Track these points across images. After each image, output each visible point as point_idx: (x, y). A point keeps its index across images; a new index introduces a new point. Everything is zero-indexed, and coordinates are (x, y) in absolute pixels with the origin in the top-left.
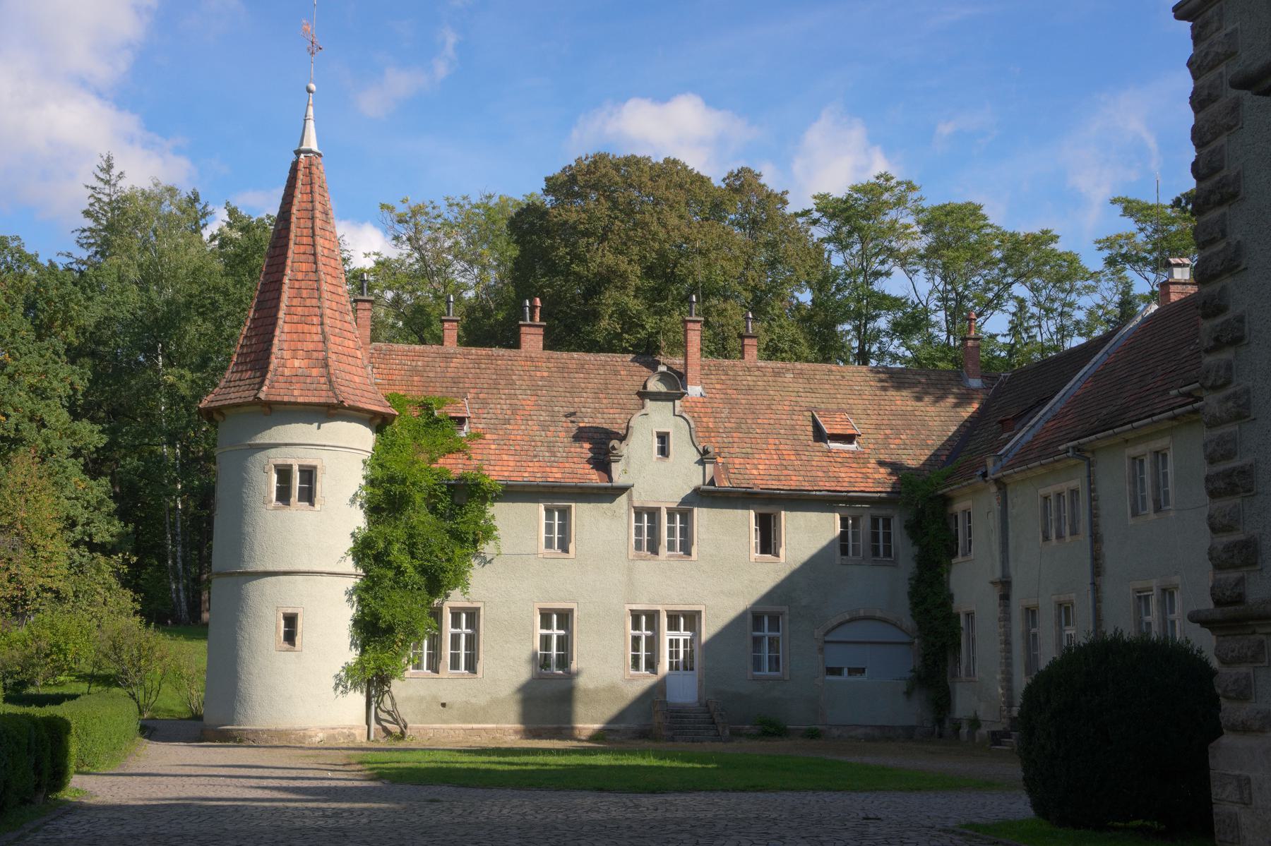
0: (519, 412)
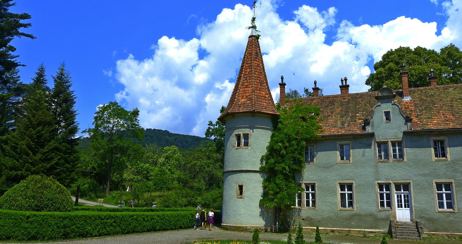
0: (334, 113)
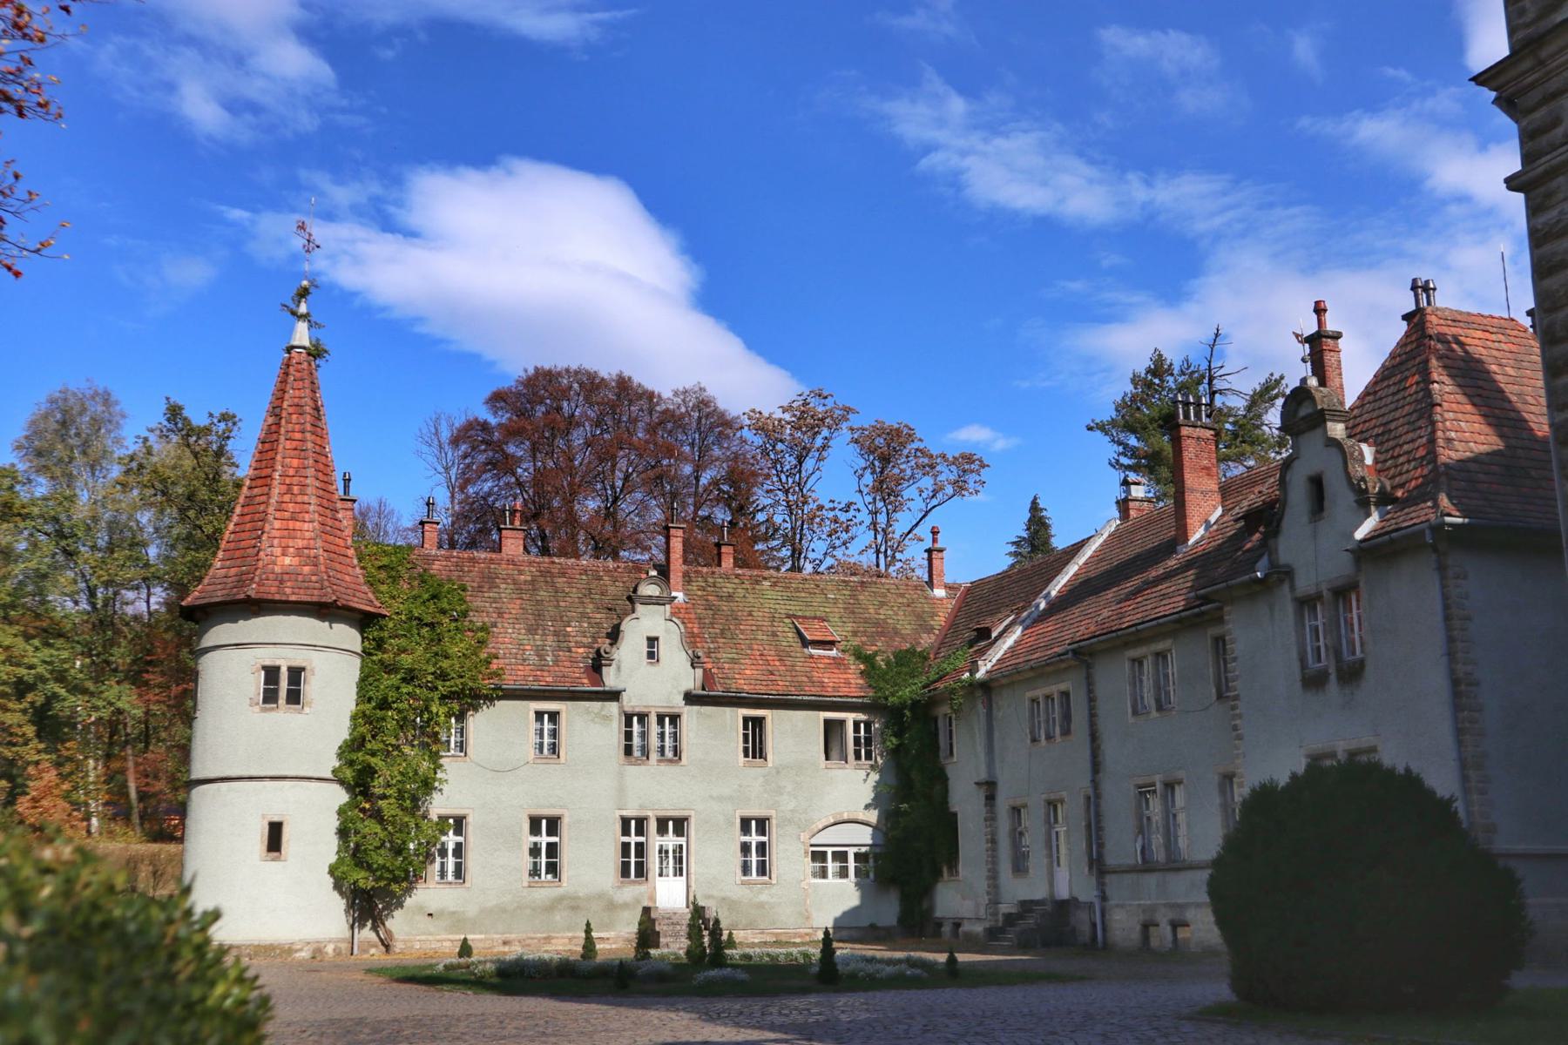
0: (506, 616)
